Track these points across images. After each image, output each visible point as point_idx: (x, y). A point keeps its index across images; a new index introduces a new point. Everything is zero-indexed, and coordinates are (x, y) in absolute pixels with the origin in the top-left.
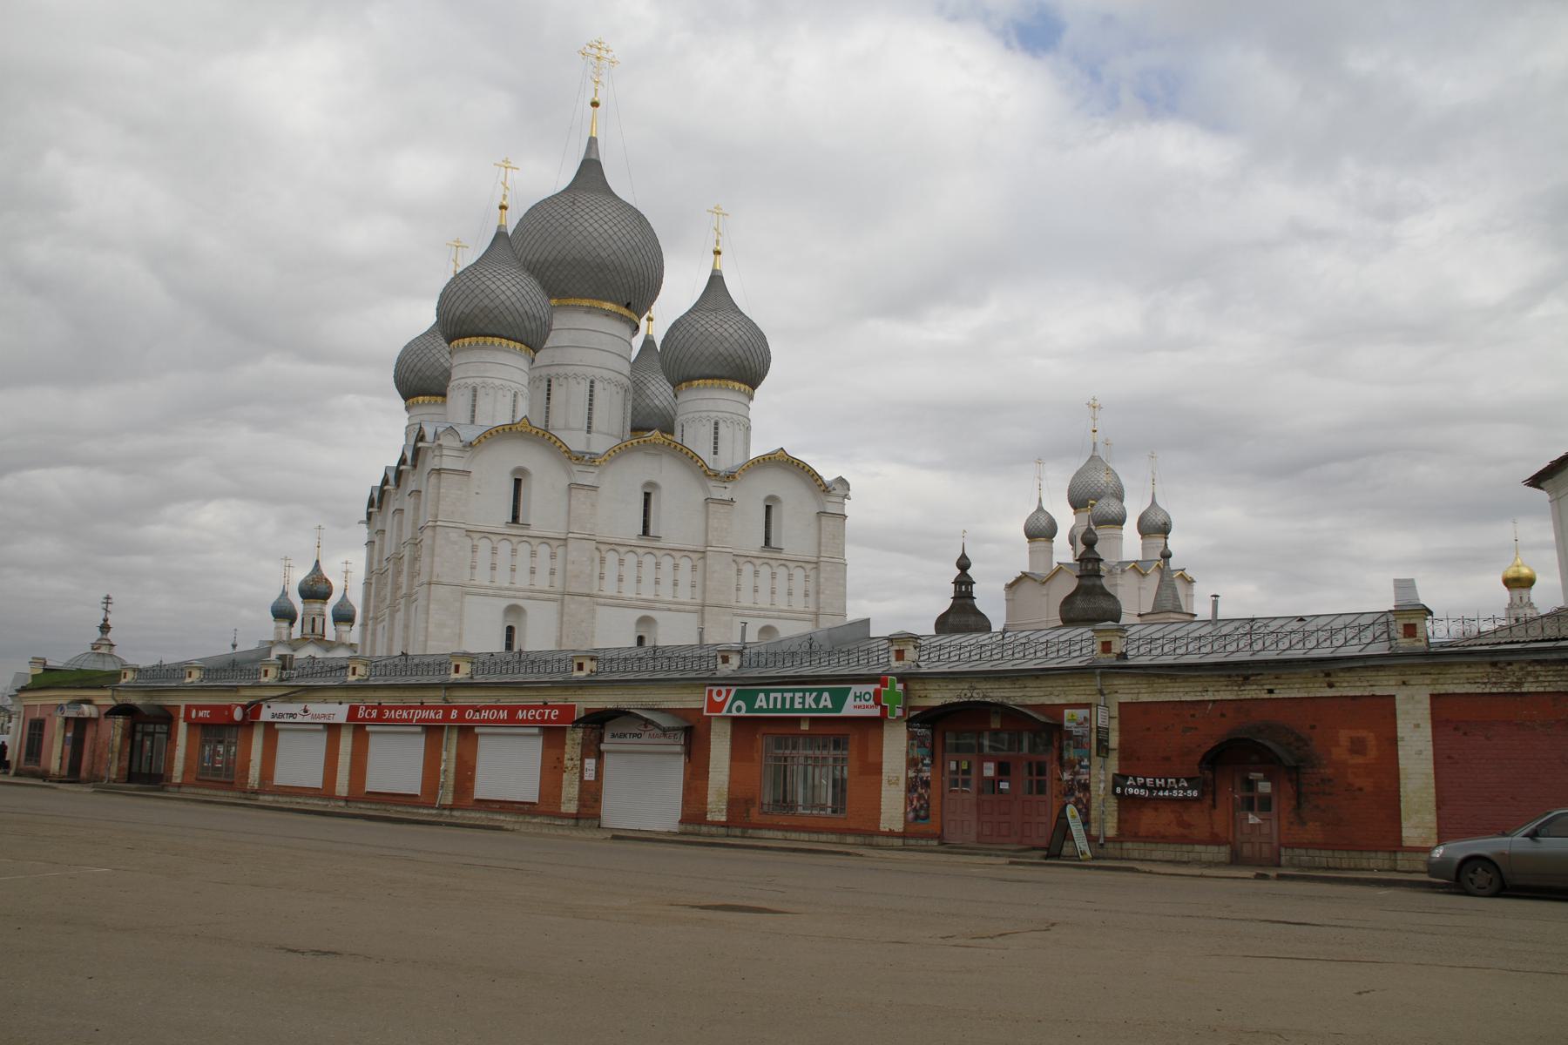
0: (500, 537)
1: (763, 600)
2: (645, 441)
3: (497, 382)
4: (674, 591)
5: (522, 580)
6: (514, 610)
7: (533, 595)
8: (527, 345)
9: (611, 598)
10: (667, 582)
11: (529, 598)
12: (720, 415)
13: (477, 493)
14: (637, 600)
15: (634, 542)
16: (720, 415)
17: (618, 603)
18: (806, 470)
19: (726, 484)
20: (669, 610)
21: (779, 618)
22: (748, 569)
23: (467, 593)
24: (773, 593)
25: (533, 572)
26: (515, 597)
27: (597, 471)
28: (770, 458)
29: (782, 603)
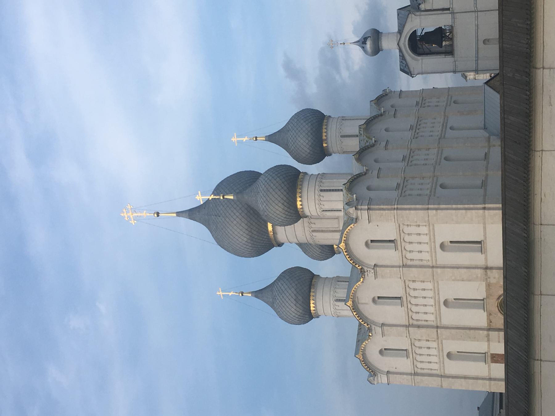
0: (415, 361)
1: (426, 248)
2: (353, 309)
3: (332, 309)
4: (428, 290)
5: (434, 352)
6: (449, 355)
7: (440, 349)
8: (310, 288)
9: (436, 318)
10: (424, 294)
11: (442, 350)
12: (318, 210)
13: (396, 368)
14: (436, 308)
15: (406, 309)
16: (318, 210)
17: (439, 314)
18: (347, 233)
19: (366, 271)
20: (438, 294)
21: (434, 242)
22: (409, 256)
23: (444, 373)
24: (420, 243)
25: (429, 348)
26: (443, 356)
27: (373, 326)
28: (346, 252)
29: (425, 239)
